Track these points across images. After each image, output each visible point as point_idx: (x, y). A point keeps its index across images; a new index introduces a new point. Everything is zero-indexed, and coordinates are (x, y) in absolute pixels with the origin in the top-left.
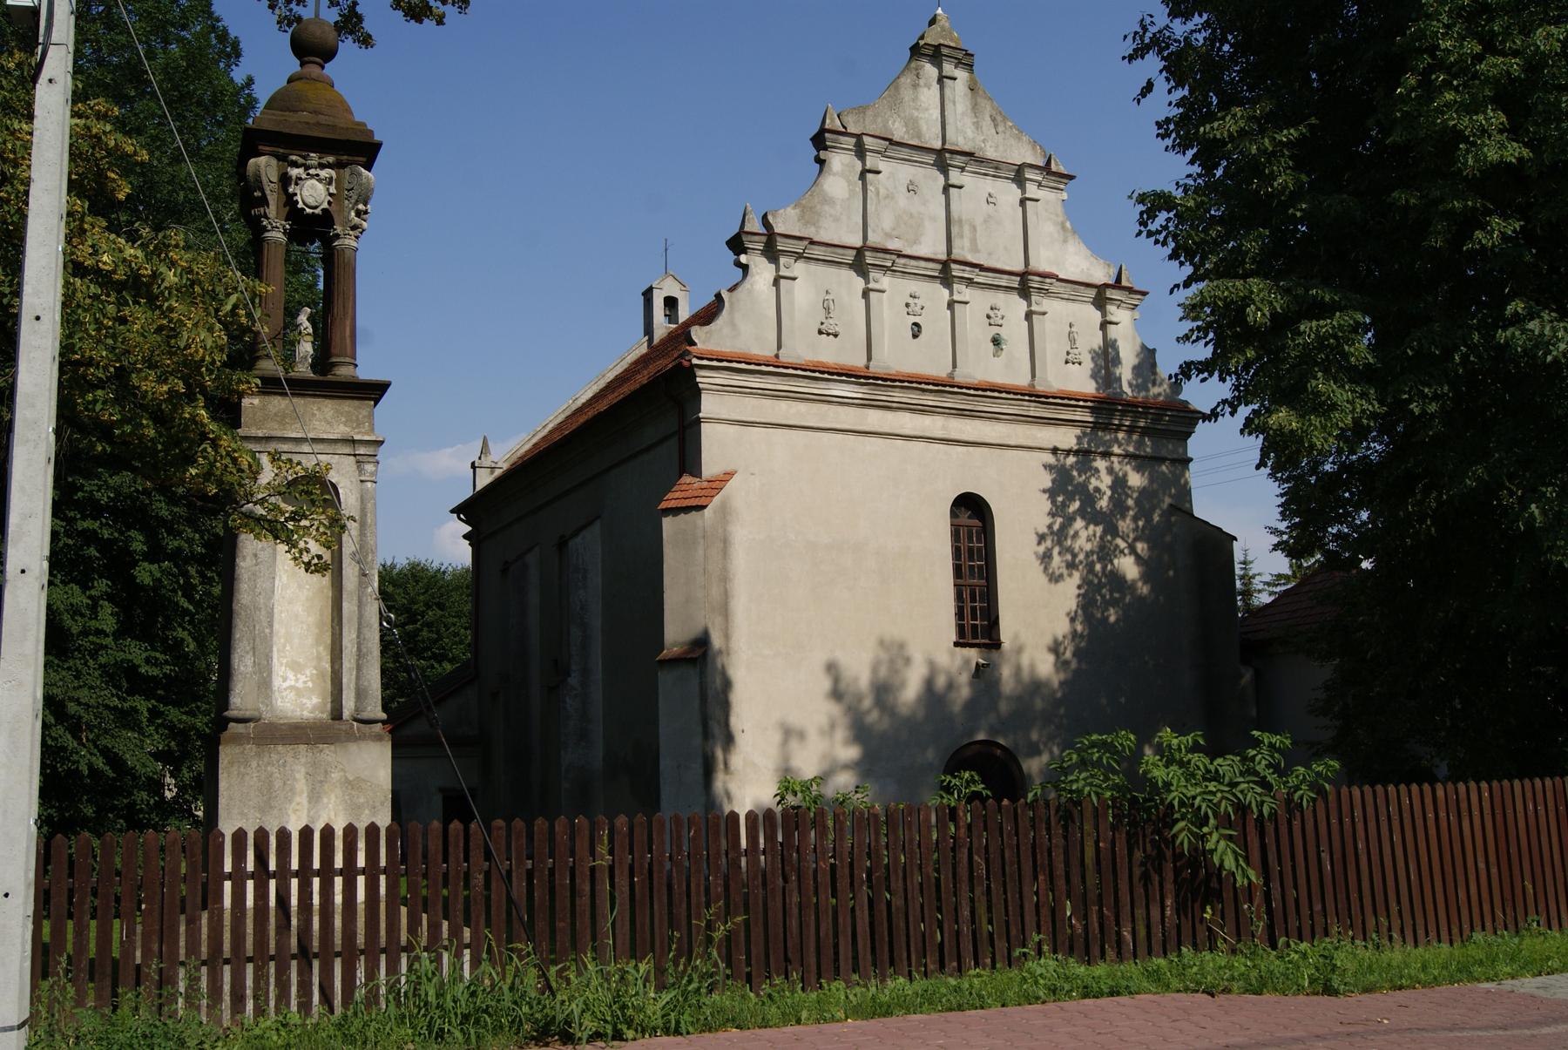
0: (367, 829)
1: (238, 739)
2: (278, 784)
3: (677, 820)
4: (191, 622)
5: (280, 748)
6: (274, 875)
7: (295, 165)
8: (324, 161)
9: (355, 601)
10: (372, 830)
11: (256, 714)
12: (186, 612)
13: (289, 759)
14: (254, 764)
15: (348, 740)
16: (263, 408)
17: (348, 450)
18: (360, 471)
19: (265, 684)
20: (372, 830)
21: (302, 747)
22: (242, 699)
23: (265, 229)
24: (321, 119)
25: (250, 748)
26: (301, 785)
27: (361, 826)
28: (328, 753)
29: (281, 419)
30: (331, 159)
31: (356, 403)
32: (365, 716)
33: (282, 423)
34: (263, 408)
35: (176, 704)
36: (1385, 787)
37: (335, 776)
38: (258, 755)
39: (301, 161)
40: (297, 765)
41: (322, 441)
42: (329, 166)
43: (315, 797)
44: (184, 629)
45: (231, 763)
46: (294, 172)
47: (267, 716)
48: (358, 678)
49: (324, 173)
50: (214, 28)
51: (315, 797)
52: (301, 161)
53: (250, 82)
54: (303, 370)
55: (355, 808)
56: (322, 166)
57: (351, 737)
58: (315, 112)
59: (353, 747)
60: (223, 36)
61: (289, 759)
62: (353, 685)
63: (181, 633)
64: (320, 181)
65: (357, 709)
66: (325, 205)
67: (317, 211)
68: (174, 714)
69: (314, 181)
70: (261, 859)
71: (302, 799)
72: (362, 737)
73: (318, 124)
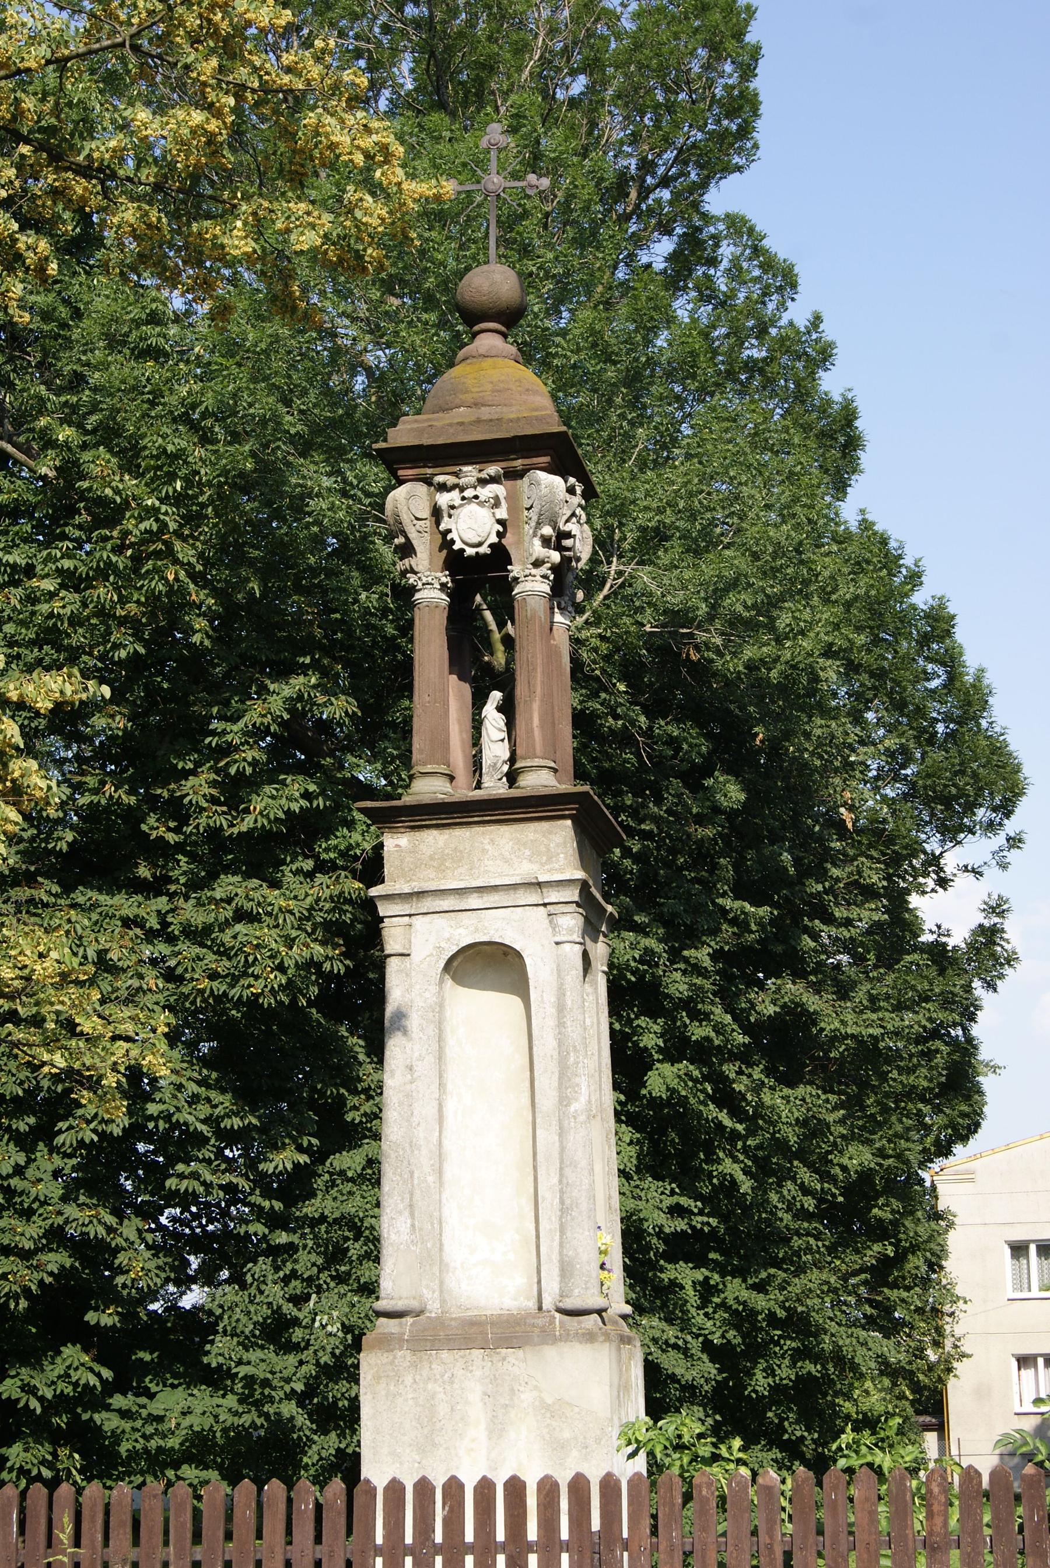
0: (386, 1489)
1: (387, 1343)
2: (443, 1409)
3: (395, 1489)
4: (745, 1150)
5: (445, 1354)
6: (567, 1547)
7: (443, 488)
8: (484, 475)
9: (555, 1128)
10: (609, 1485)
11: (414, 1304)
12: (734, 1136)
13: (459, 1373)
14: (408, 1380)
15: (544, 1342)
16: (413, 850)
17: (534, 898)
18: (553, 926)
19: (434, 1259)
20: (609, 1485)
21: (477, 1353)
22: (397, 1279)
23: (413, 590)
24: (485, 413)
25: (403, 1356)
26: (477, 1412)
27: (564, 1480)
28: (515, 1362)
29: (439, 862)
30: (493, 469)
31: (545, 825)
32: (569, 1304)
33: (441, 869)
34: (413, 850)
35: (741, 1273)
36: (260, 1484)
37: (527, 1397)
38: (414, 1365)
39: (450, 480)
40: (466, 1380)
41: (495, 888)
42: (493, 480)
43: (497, 1429)
44: (736, 1160)
45: (377, 1378)
46: (444, 499)
47: (434, 1308)
48: (561, 1245)
49: (486, 492)
50: (757, 251)
51: (497, 1429)
52: (450, 480)
53: (817, 320)
54: (494, 786)
55: (558, 1447)
56: (483, 482)
57: (548, 1337)
58: (476, 405)
59: (550, 1352)
60: (769, 264)
61: (459, 1373)
62: (555, 1257)
63: (729, 1167)
64: (482, 504)
65: (562, 1296)
66: (494, 539)
67: (484, 549)
68: (735, 1290)
69: (473, 507)
70: (455, 1521)
71: (478, 1432)
72: (566, 1337)
73: (479, 421)
